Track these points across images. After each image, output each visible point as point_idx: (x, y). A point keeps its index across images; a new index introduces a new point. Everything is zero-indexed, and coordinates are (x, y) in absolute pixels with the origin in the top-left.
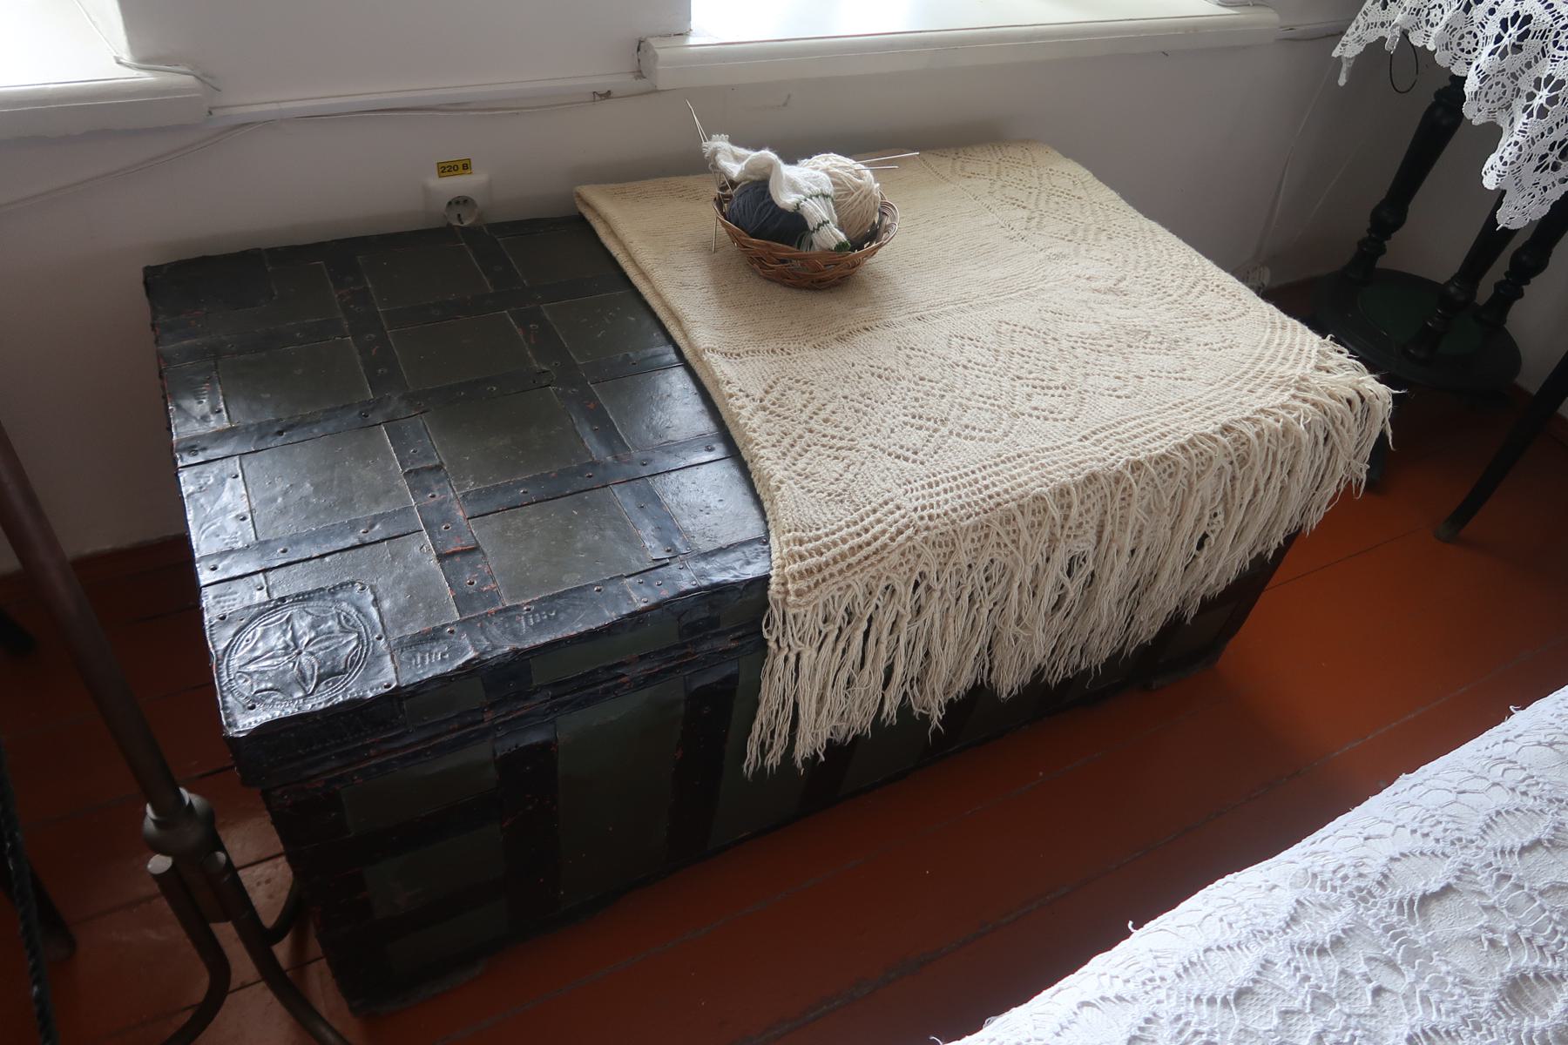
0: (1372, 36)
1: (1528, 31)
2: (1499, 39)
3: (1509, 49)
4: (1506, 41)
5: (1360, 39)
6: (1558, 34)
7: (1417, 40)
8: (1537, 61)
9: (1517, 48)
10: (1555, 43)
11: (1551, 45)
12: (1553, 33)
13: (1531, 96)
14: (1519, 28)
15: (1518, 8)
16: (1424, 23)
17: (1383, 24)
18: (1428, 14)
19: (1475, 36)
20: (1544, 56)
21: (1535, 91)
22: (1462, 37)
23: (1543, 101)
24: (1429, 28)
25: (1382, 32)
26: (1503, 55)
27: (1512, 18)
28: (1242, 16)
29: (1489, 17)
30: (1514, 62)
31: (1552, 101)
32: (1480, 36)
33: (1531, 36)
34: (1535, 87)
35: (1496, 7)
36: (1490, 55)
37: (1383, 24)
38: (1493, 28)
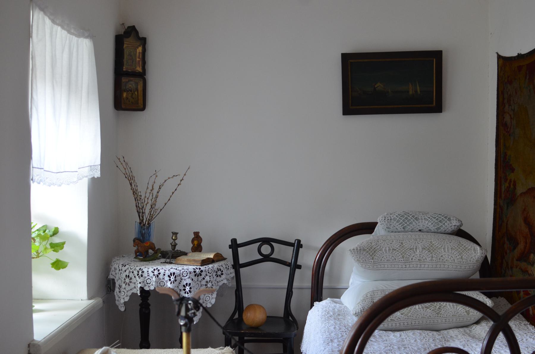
0: (130, 293)
1: (176, 276)
2: (170, 280)
3: (174, 281)
4: (172, 280)
5: (127, 296)
6: (182, 274)
7: (147, 288)
8: (181, 282)
9: (176, 280)
10: (183, 276)
11: (182, 277)
12: (181, 274)
13: (184, 290)
14: (174, 276)
15: (170, 272)
16: (146, 284)
17: (131, 290)
18: (146, 282)
19: (163, 282)
20: (182, 280)
21: (185, 288)
22: (160, 283)
23: (189, 289)
24: (149, 285)
25: (132, 291)
26: (174, 283)
27: (170, 274)
28: (95, 301)
29: (164, 276)
30: (176, 283)
31: (190, 288)
32: (164, 281)
33: (177, 277)
34: (184, 287)
35: (165, 273)
36: (171, 284)
37: (131, 290)
38: (167, 278)
